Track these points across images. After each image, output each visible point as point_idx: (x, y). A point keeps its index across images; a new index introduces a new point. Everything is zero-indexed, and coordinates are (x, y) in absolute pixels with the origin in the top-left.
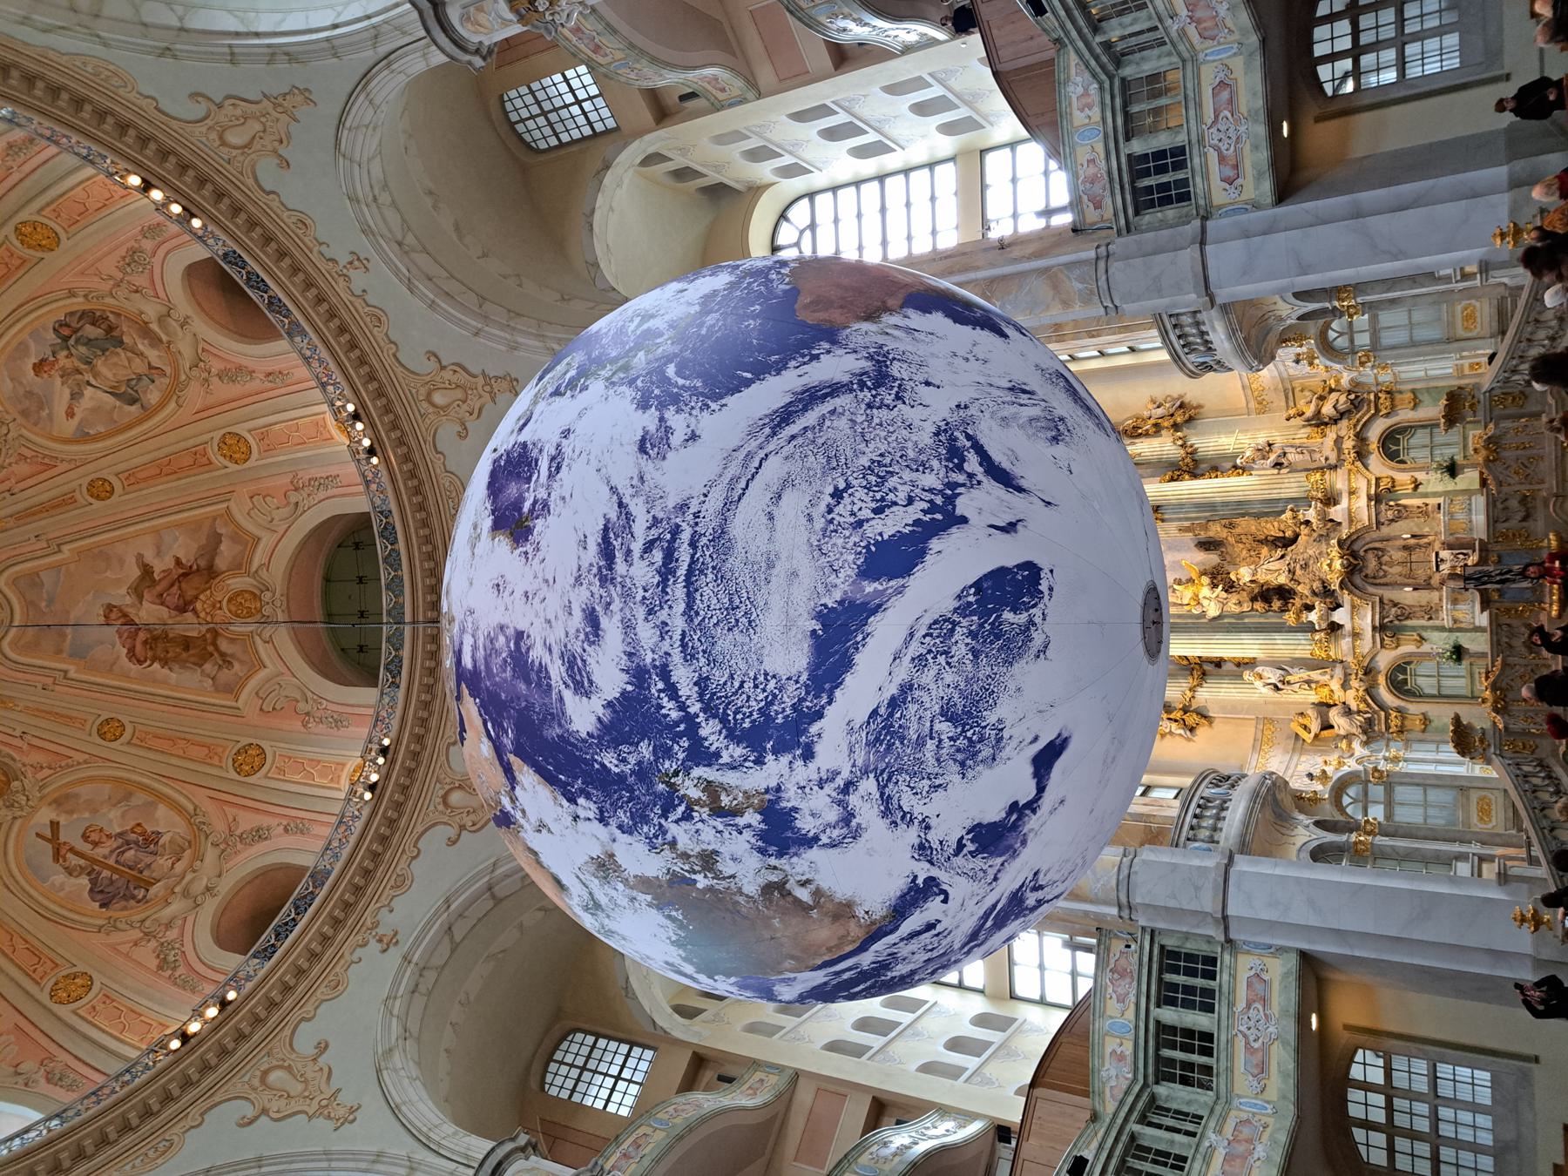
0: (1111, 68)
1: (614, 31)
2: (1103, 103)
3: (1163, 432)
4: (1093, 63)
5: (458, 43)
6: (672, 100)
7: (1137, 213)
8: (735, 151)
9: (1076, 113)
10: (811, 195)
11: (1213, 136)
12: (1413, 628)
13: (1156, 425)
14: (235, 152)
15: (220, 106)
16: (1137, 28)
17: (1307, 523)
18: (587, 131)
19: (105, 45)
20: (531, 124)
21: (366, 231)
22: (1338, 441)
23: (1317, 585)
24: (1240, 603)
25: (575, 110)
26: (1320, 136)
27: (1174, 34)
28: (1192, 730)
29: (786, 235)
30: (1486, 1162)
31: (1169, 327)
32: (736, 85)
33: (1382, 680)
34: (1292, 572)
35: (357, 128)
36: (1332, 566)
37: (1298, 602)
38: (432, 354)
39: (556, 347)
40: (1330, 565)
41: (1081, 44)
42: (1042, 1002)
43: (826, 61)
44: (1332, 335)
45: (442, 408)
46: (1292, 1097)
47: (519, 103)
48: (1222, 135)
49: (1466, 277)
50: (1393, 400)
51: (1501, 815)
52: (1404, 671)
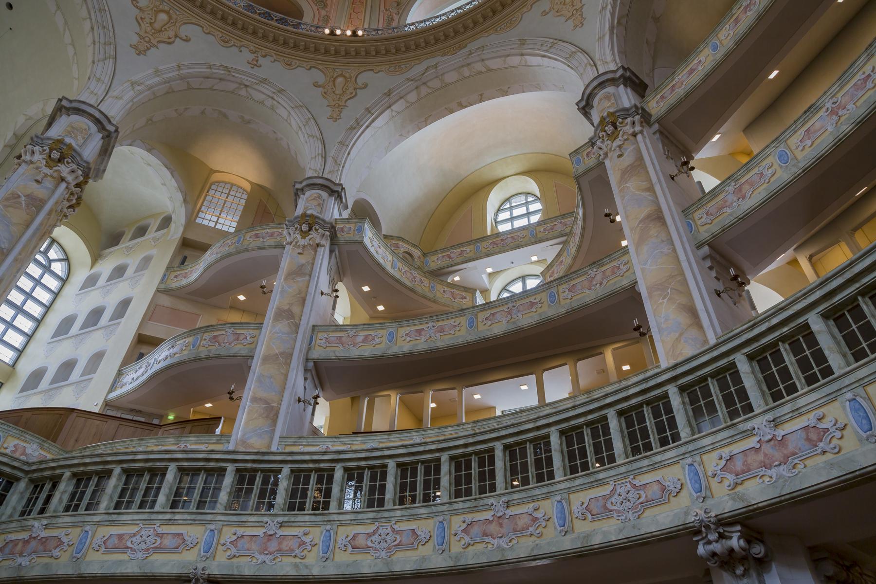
1: (259, 248)
5: (312, 186)
6: (188, 252)
9: (16, 442)
14: (336, 75)
15: (355, 89)
16: (55, 501)
19: (408, 79)
21: (264, 81)
27: (30, 523)
35: (307, 122)
39: (139, 88)
47: (239, 195)
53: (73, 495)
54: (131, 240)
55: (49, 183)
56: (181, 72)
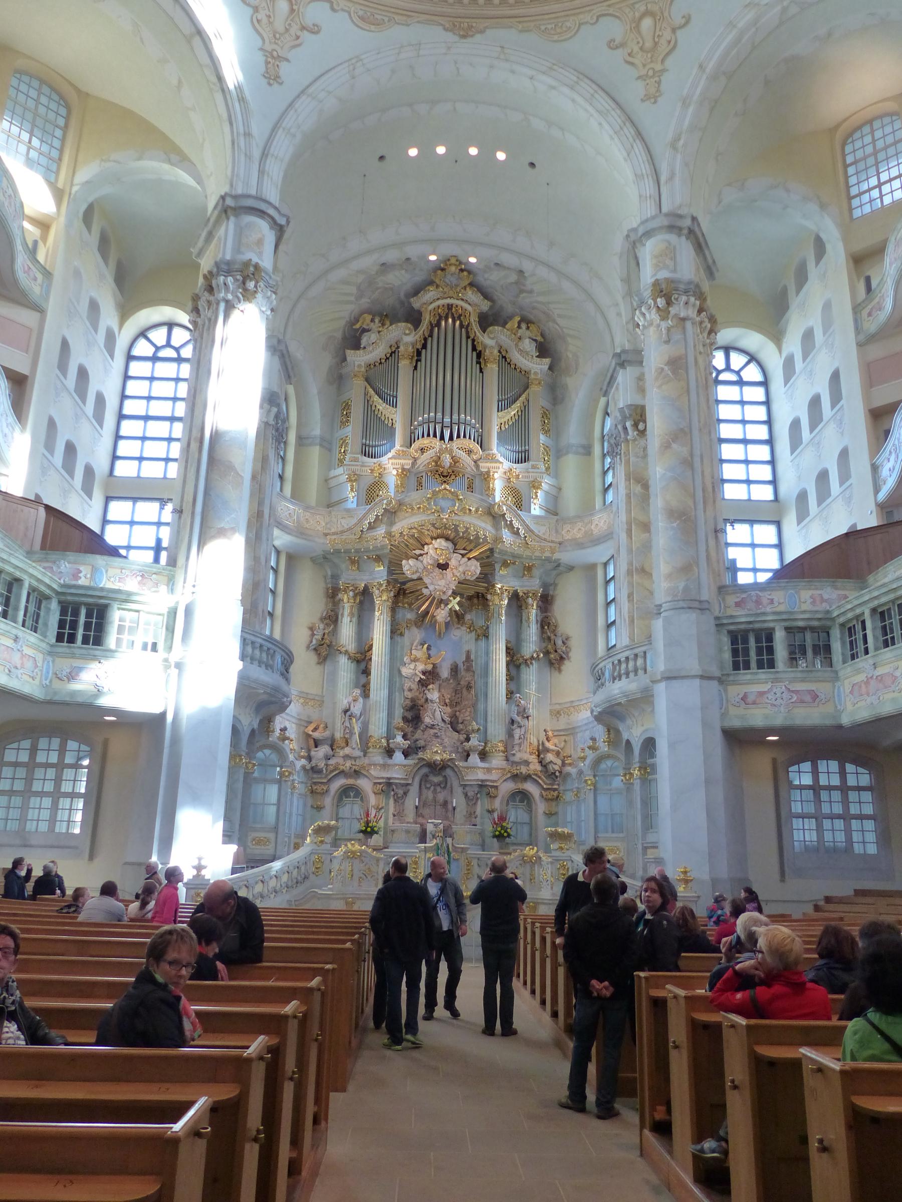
0: (842, 620)
2: (817, 612)
3: (544, 645)
4: (849, 606)
7: (729, 632)
8: (815, 321)
9: (810, 593)
10: (765, 384)
11: (779, 688)
12: (387, 804)
13: (549, 638)
17: (468, 739)
18: (854, 191)
20: (868, 139)
22: (527, 763)
23: (421, 743)
24: (410, 690)
25: (873, 182)
26: (761, 762)
27: (861, 665)
28: (315, 649)
29: (737, 360)
30: (12, 826)
31: (636, 651)
32: (871, 326)
33: (350, 781)
34: (432, 727)
36: (436, 753)
37: (409, 730)
38: (688, 20)
39: (681, 142)
40: (436, 752)
41: (866, 598)
42: (105, 522)
43: (878, 403)
44: (609, 763)
45: (638, 27)
46: (56, 698)
47: (888, 129)
48: (778, 695)
49: (645, 849)
50: (552, 800)
51: (257, 852)
52: (355, 796)
53: (884, 628)
54: (798, 291)
55: (677, 336)
56: (708, 70)
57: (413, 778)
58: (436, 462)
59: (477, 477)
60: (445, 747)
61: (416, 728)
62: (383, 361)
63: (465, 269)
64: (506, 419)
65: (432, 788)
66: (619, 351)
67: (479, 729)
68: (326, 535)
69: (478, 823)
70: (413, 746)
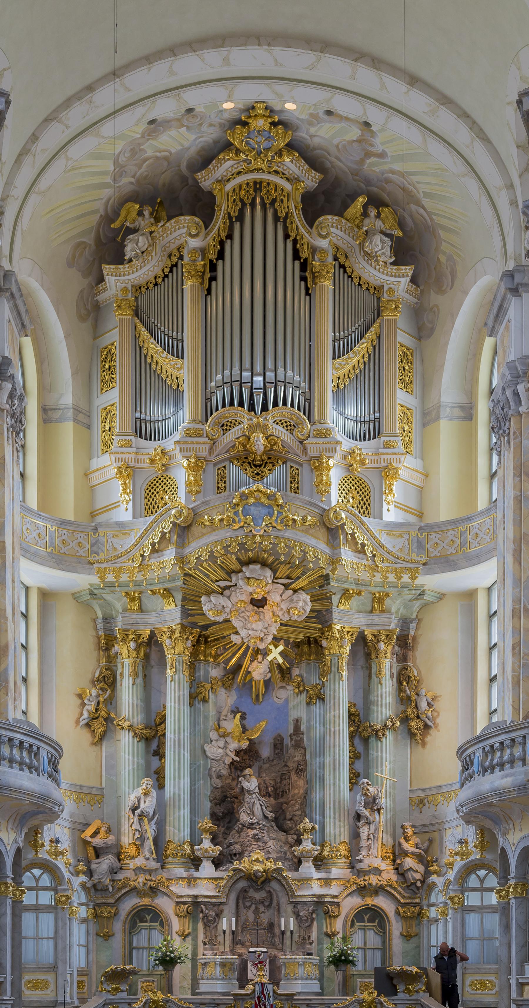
23: (237, 848)
34: (251, 826)
40: (257, 860)
57: (227, 895)
58: (245, 446)
59: (305, 465)
60: (269, 852)
61: (229, 829)
62: (160, 280)
63: (280, 123)
64: (345, 371)
65: (253, 906)
66: (511, 269)
67: (313, 828)
68: (91, 564)
69: (313, 951)
70: (226, 852)
